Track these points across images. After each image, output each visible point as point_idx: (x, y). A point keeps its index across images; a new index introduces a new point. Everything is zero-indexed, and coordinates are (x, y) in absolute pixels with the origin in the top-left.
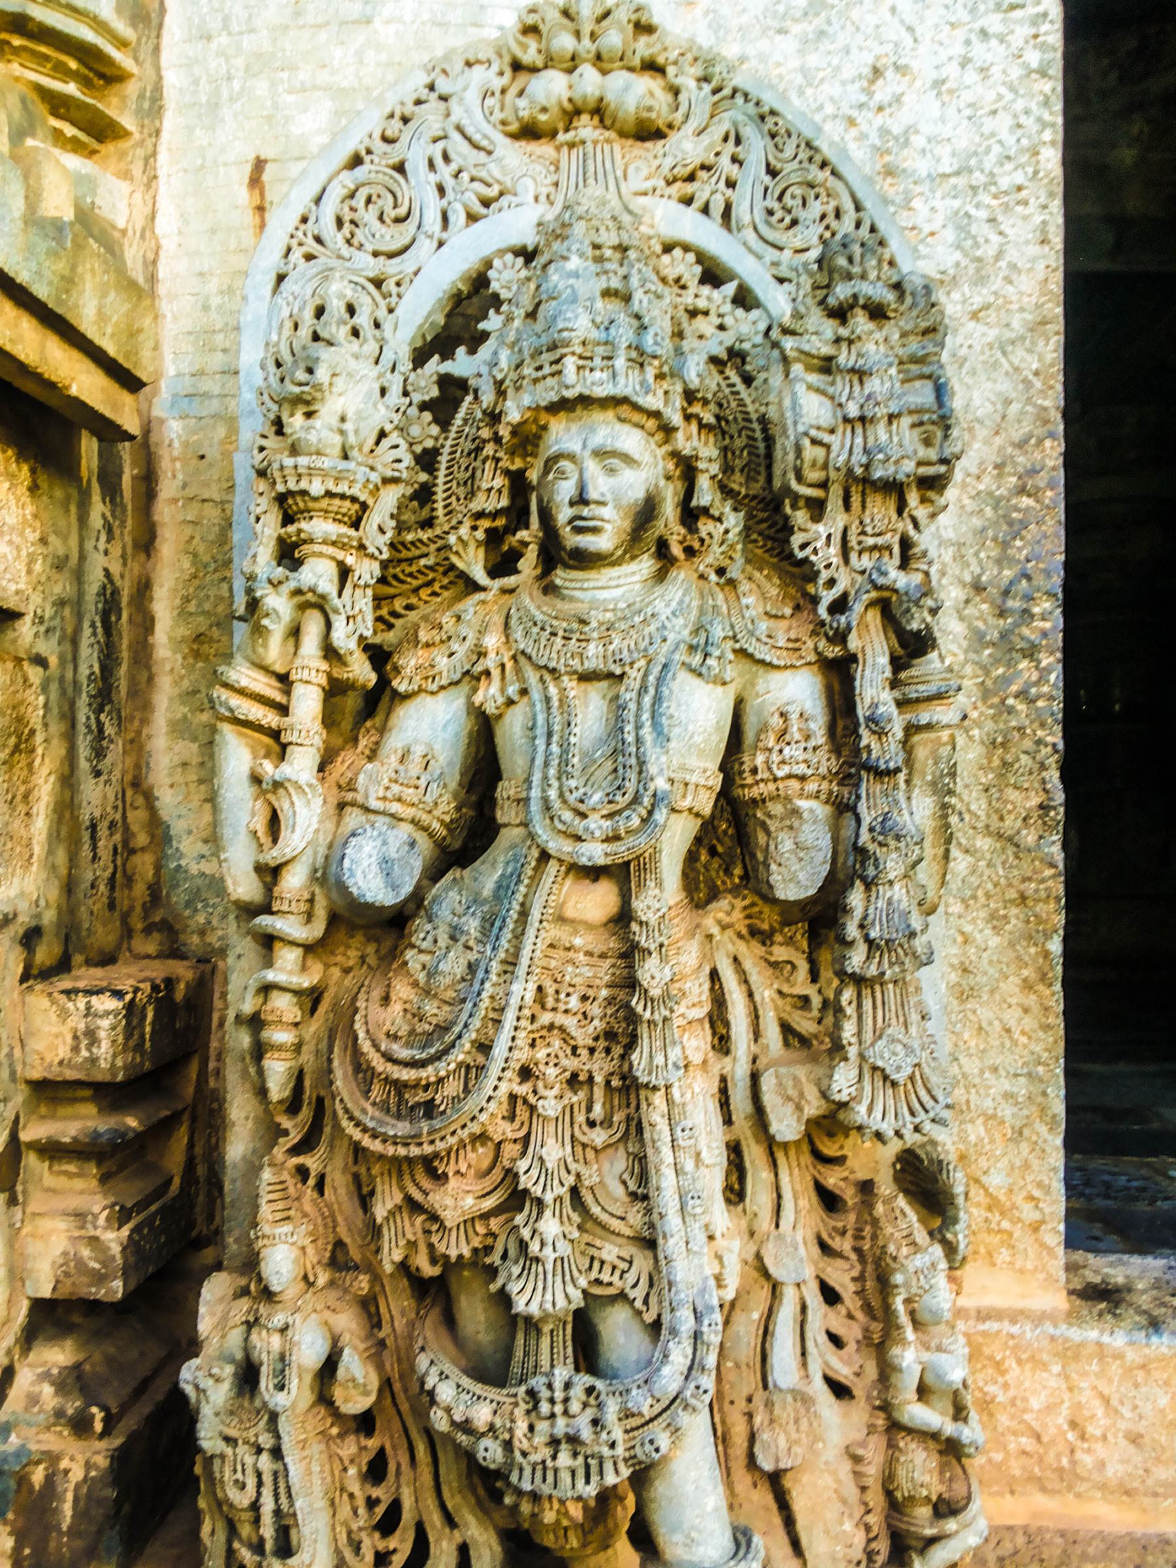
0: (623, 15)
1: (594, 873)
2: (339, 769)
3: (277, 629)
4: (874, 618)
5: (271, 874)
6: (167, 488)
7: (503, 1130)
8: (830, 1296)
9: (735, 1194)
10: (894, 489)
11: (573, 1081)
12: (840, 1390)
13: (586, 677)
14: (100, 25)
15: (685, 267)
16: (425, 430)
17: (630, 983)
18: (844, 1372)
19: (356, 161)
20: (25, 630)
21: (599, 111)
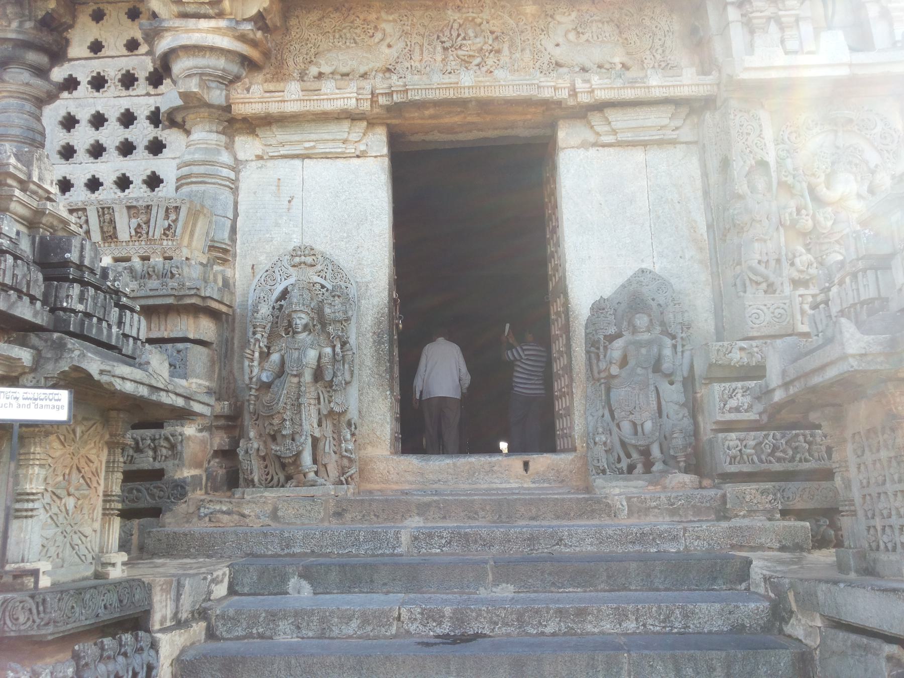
0: (308, 248)
1: (295, 376)
2: (262, 364)
3: (252, 344)
4: (338, 339)
5: (251, 379)
6: (237, 321)
7: (282, 411)
8: (334, 439)
9: (320, 425)
10: (340, 322)
11: (292, 405)
12: (335, 453)
13: (295, 349)
14: (225, 244)
15: (318, 286)
16: (277, 313)
17: (300, 390)
18: (336, 450)
19: (267, 271)
20: (214, 345)
21: (304, 263)
